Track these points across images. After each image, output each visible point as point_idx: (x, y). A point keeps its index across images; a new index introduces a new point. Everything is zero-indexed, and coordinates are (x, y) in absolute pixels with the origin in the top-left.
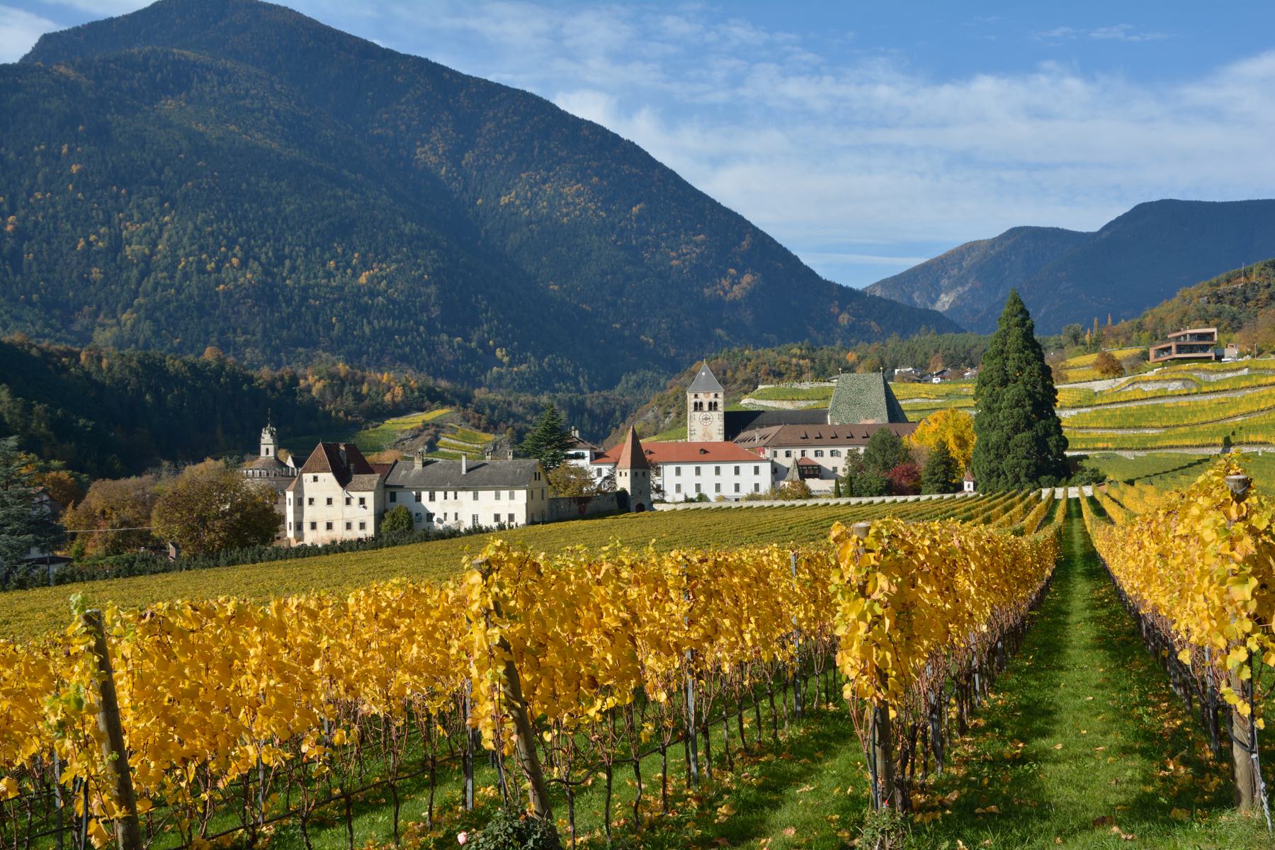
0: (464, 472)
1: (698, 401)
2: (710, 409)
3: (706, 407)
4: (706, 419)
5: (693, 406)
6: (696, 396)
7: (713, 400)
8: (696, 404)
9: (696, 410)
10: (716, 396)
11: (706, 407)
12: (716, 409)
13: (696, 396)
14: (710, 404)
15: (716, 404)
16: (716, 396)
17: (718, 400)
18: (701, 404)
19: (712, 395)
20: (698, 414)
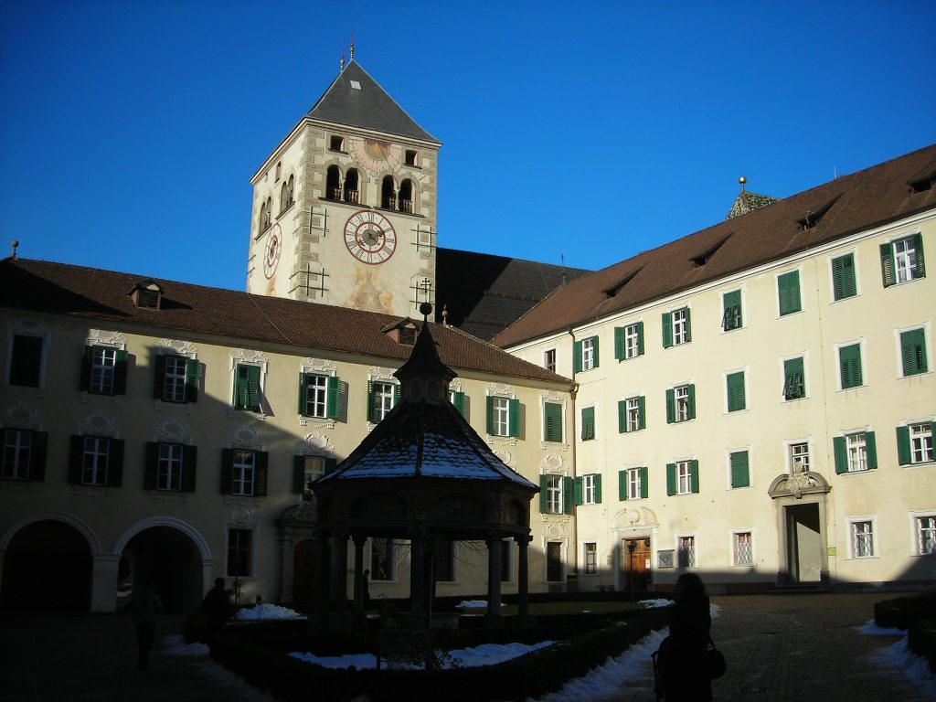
1: (345, 162)
2: (386, 205)
3: (370, 192)
4: (371, 237)
5: (321, 178)
6: (336, 144)
7: (401, 173)
8: (333, 172)
9: (330, 196)
10: (410, 158)
11: (370, 192)
13: (336, 144)
14: (387, 183)
17: (416, 174)
18: (352, 176)
19: (397, 152)
20: (338, 213)
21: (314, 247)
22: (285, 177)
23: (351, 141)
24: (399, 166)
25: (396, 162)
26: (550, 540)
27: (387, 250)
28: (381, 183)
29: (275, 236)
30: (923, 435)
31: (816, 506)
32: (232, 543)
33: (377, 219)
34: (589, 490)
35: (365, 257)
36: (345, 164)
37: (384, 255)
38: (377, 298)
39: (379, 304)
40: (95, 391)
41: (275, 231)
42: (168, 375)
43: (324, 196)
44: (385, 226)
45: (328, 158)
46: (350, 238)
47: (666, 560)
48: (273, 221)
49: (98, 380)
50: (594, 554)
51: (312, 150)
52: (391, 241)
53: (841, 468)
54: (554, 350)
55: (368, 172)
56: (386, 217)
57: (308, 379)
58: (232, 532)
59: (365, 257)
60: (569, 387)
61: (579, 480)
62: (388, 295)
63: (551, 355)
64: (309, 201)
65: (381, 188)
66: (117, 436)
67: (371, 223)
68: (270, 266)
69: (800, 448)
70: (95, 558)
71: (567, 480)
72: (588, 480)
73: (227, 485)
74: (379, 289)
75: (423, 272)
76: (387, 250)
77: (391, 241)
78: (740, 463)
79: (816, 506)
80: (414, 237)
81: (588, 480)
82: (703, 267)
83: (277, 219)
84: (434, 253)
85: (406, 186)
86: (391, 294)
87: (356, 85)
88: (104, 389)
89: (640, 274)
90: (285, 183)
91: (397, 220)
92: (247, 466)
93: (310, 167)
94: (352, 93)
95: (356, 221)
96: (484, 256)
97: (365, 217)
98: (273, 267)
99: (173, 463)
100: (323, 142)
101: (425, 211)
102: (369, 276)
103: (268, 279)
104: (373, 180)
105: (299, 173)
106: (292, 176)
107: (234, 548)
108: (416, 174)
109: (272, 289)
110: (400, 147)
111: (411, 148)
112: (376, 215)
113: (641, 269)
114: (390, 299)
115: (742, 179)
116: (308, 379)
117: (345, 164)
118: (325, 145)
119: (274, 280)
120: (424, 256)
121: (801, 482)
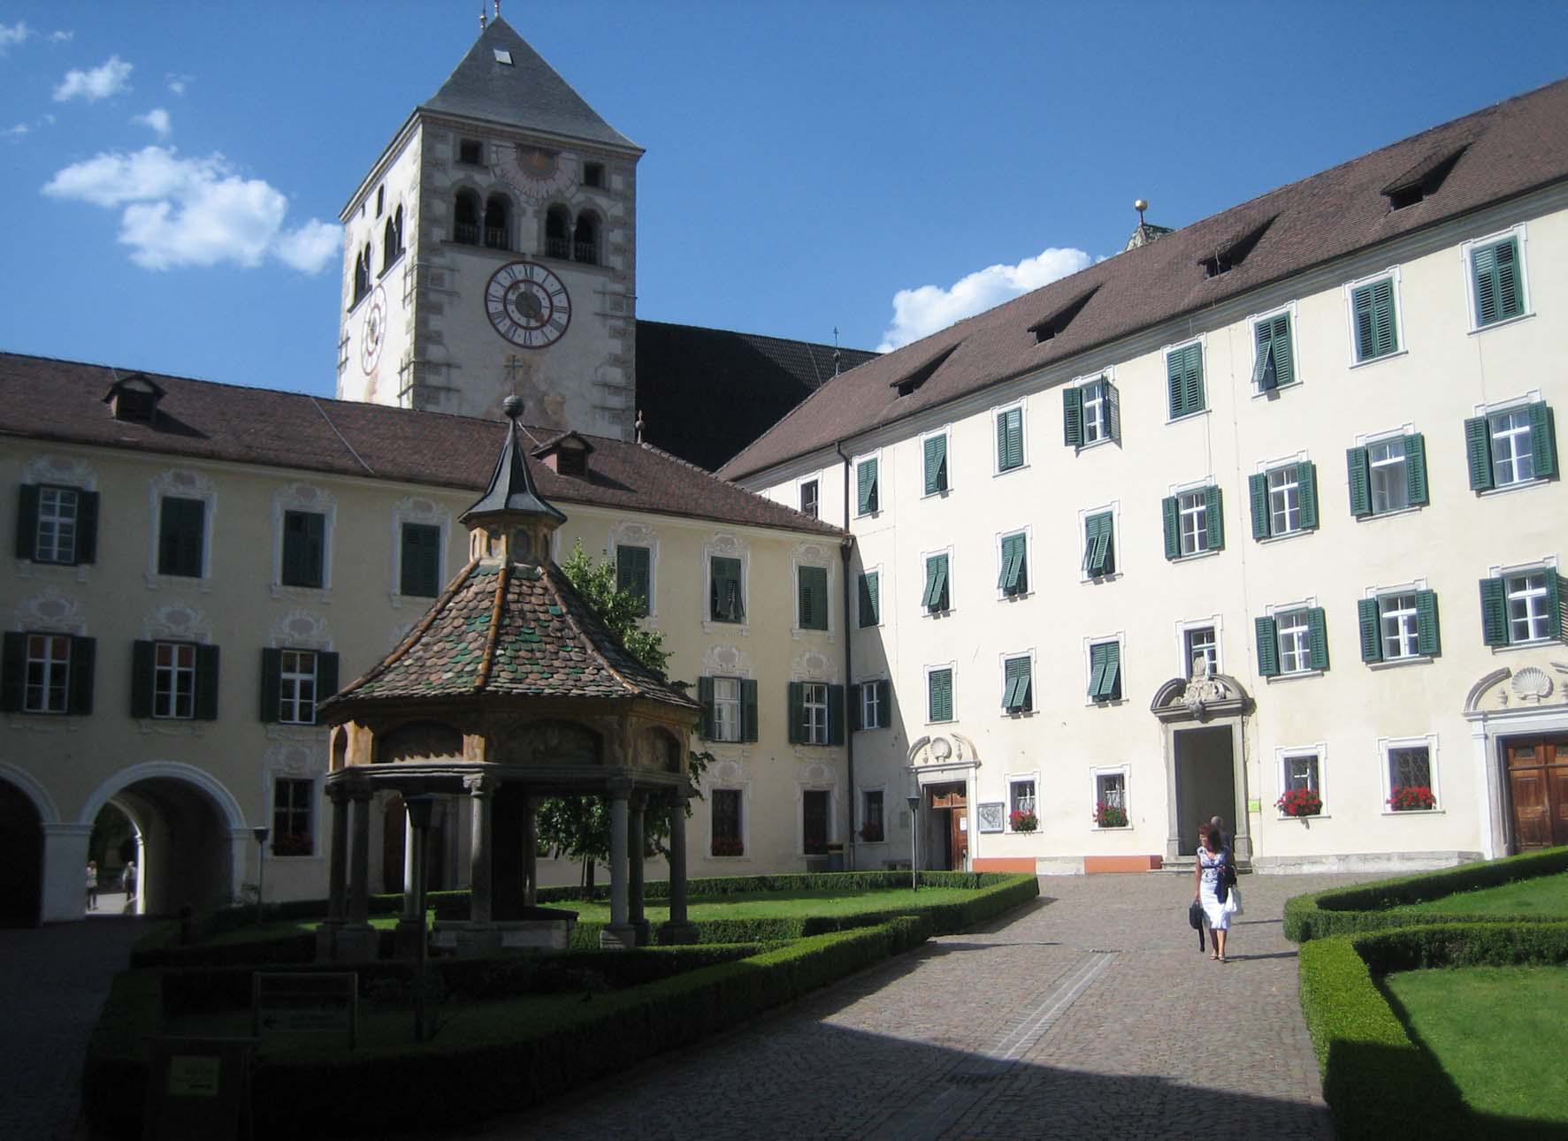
1: (483, 182)
3: (529, 232)
5: (444, 209)
6: (471, 154)
7: (577, 199)
8: (465, 203)
10: (593, 176)
11: (529, 232)
14: (555, 220)
17: (602, 202)
18: (500, 210)
19: (569, 168)
20: (474, 267)
21: (435, 323)
22: (390, 211)
23: (494, 149)
24: (573, 189)
25: (569, 183)
26: (809, 788)
27: (556, 325)
28: (545, 216)
29: (377, 306)
30: (1402, 614)
31: (1228, 730)
32: (281, 799)
33: (539, 274)
34: (871, 707)
35: (520, 337)
36: (485, 186)
37: (553, 334)
38: (540, 401)
39: (544, 412)
40: (46, 559)
41: (376, 296)
42: (43, 518)
43: (451, 237)
44: (553, 286)
45: (453, 177)
46: (495, 307)
47: (990, 819)
48: (374, 281)
49: (48, 541)
50: (880, 810)
51: (429, 165)
52: (561, 310)
53: (1271, 664)
54: (816, 482)
55: (523, 198)
56: (554, 271)
57: (29, 497)
58: (281, 786)
59: (520, 337)
60: (838, 541)
61: (854, 691)
62: (559, 399)
63: (810, 492)
64: (425, 247)
65: (543, 224)
66: (84, 633)
67: (529, 281)
68: (370, 354)
69: (1199, 638)
70: (48, 831)
71: (835, 691)
72: (870, 690)
73: (272, 706)
74: (543, 387)
75: (616, 361)
76: (556, 325)
77: (561, 310)
78: (1105, 655)
79: (1228, 730)
81: (870, 690)
82: (1049, 342)
83: (379, 277)
84: (632, 329)
85: (589, 224)
86: (563, 397)
87: (504, 57)
88: (61, 555)
89: (954, 355)
90: (390, 219)
91: (578, 279)
92: (306, 677)
93: (428, 190)
94: (497, 69)
95: (505, 279)
96: (719, 332)
97: (519, 271)
98: (375, 356)
99: (180, 673)
101: (616, 261)
102: (528, 368)
103: (368, 374)
104: (530, 211)
105: (412, 202)
106: (400, 209)
107: (284, 810)
108: (602, 202)
109: (373, 392)
110: (573, 156)
111: (594, 159)
112: (537, 269)
113: (955, 348)
114: (562, 404)
115: (1138, 203)
116: (29, 497)
117: (485, 186)
118: (451, 154)
119: (376, 376)
120: (617, 333)
121: (1200, 692)
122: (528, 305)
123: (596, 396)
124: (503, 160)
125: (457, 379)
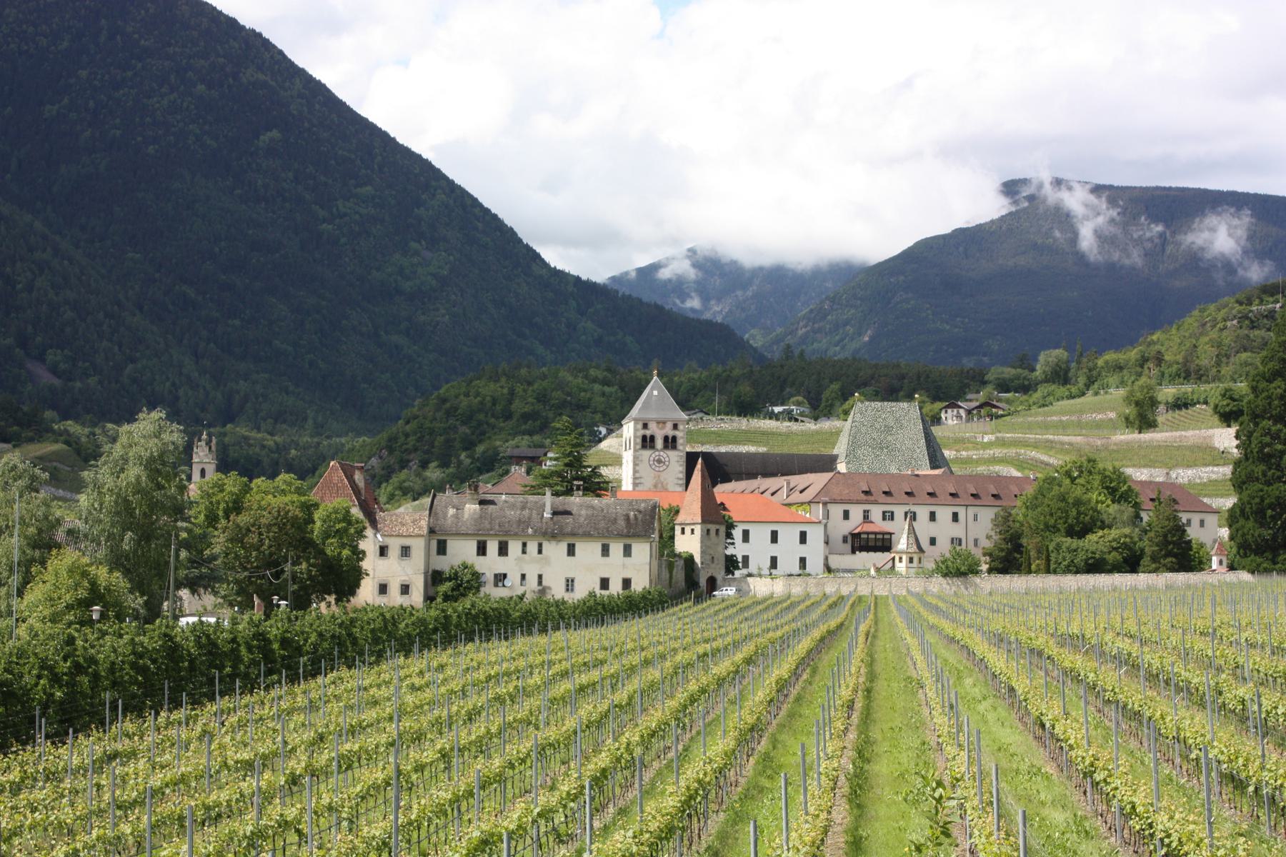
0: (547, 515)
1: (648, 433)
3: (659, 443)
4: (659, 461)
5: (639, 440)
6: (645, 426)
7: (671, 433)
8: (644, 438)
9: (644, 446)
10: (675, 427)
11: (659, 443)
12: (674, 447)
14: (666, 438)
15: (674, 438)
16: (675, 427)
17: (677, 433)
18: (652, 438)
19: (669, 425)
20: (646, 453)
21: (637, 468)
45: (642, 432)
51: (636, 430)
80: (676, 459)
91: (672, 453)
100: (640, 426)
122: (659, 461)
123: (676, 481)
124: (652, 426)
125: (642, 480)
